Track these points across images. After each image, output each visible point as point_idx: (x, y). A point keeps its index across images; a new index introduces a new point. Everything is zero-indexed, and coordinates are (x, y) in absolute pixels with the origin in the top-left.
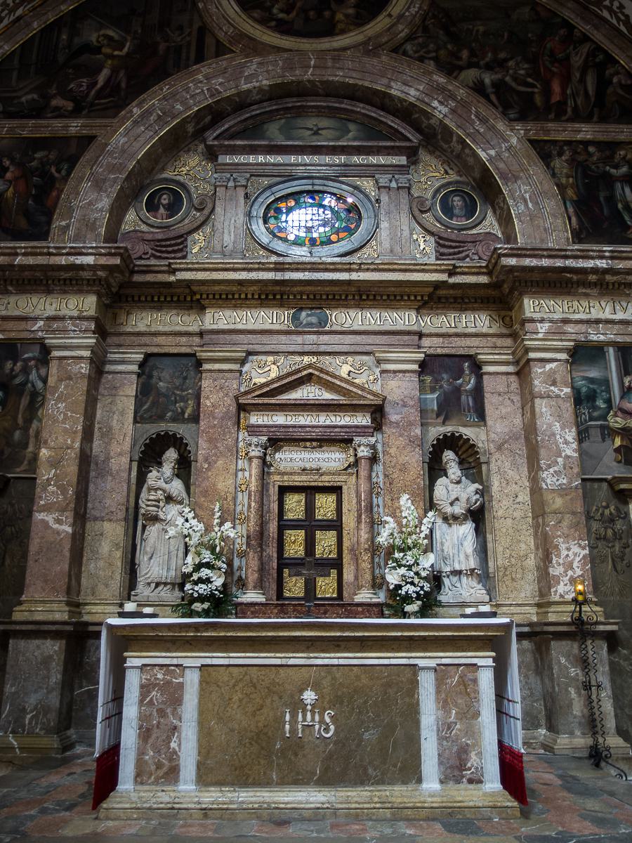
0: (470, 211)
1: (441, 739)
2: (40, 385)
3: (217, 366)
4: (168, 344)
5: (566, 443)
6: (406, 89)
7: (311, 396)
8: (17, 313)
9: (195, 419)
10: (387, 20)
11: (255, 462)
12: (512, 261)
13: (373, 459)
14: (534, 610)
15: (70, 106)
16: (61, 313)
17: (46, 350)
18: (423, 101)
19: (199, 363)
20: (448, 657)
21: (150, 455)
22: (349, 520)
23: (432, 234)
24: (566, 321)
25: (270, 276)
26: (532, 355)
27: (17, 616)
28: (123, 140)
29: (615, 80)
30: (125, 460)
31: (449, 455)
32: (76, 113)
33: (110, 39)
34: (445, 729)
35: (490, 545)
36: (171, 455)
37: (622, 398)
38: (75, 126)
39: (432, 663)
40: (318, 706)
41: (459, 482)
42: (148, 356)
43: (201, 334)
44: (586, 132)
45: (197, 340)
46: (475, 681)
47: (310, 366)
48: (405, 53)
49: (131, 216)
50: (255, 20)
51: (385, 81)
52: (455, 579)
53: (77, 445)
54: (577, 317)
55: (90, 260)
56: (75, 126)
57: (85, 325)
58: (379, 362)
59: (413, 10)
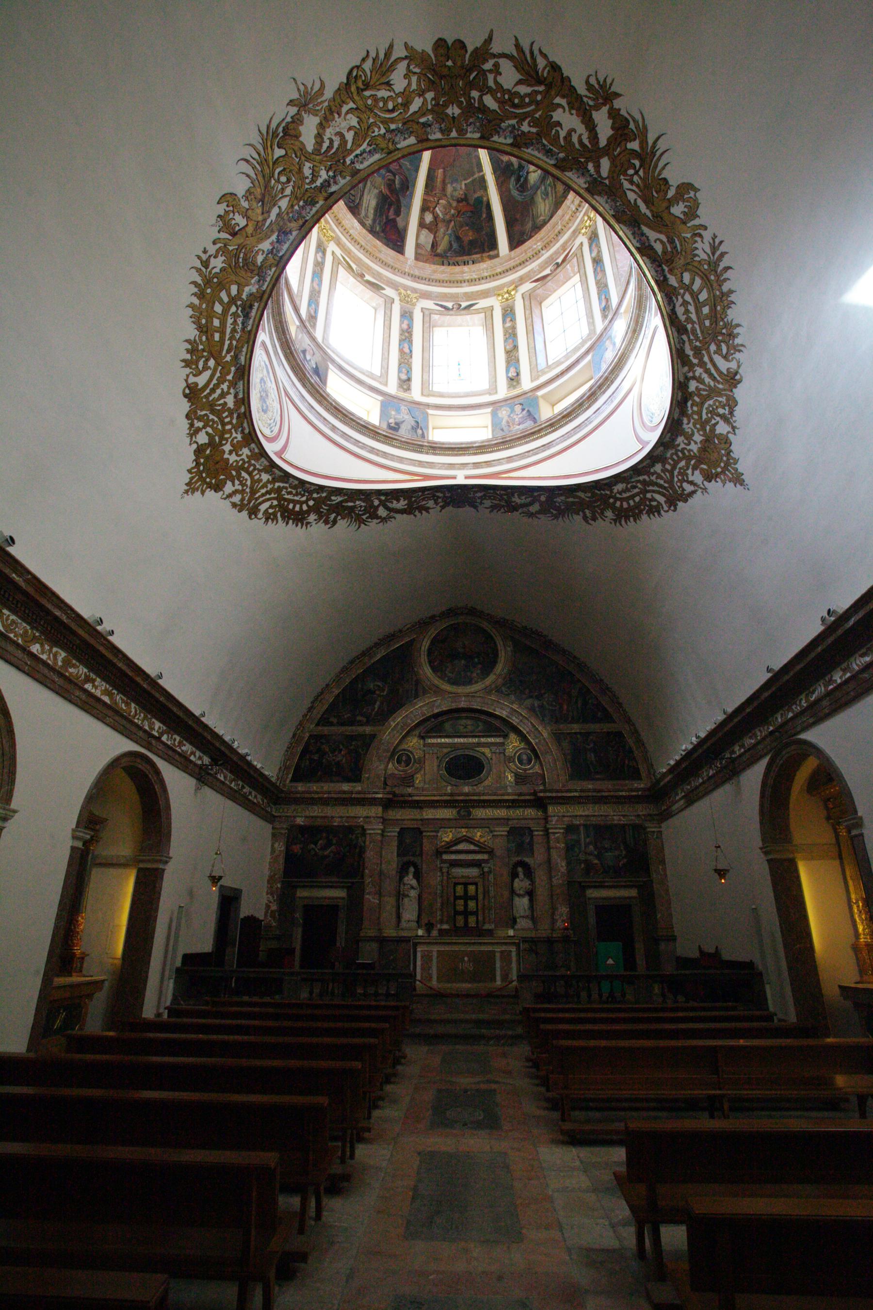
0: (530, 761)
1: (501, 971)
2: (363, 844)
3: (428, 834)
4: (409, 825)
5: (562, 866)
6: (501, 711)
7: (465, 848)
8: (352, 815)
9: (421, 855)
10: (494, 677)
11: (445, 874)
12: (541, 794)
13: (490, 872)
14: (550, 931)
15: (365, 720)
16: (370, 814)
17: (364, 830)
18: (508, 717)
19: (421, 833)
20: (504, 948)
21: (403, 871)
22: (480, 897)
23: (512, 772)
24: (564, 816)
25: (448, 798)
26: (550, 831)
27: (362, 935)
28: (388, 738)
29: (590, 701)
30: (394, 872)
31: (520, 869)
32: (367, 723)
33: (379, 686)
34: (502, 968)
35: (534, 906)
36: (412, 869)
37: (585, 847)
38: (368, 729)
39: (499, 950)
40: (469, 961)
41: (522, 881)
42: (401, 829)
43: (421, 820)
44: (576, 728)
45: (420, 822)
46: (511, 955)
47: (465, 836)
48: (502, 692)
49: (390, 766)
50: (439, 677)
51: (493, 707)
52: (521, 919)
53: (378, 869)
54: (569, 814)
55: (380, 796)
56: (368, 729)
57: (379, 820)
58: (491, 832)
59: (505, 671)
